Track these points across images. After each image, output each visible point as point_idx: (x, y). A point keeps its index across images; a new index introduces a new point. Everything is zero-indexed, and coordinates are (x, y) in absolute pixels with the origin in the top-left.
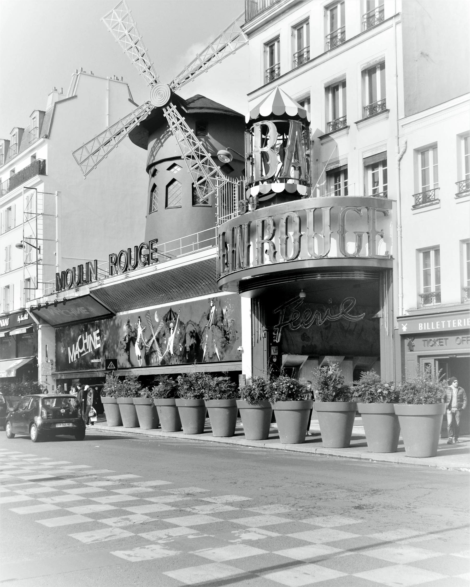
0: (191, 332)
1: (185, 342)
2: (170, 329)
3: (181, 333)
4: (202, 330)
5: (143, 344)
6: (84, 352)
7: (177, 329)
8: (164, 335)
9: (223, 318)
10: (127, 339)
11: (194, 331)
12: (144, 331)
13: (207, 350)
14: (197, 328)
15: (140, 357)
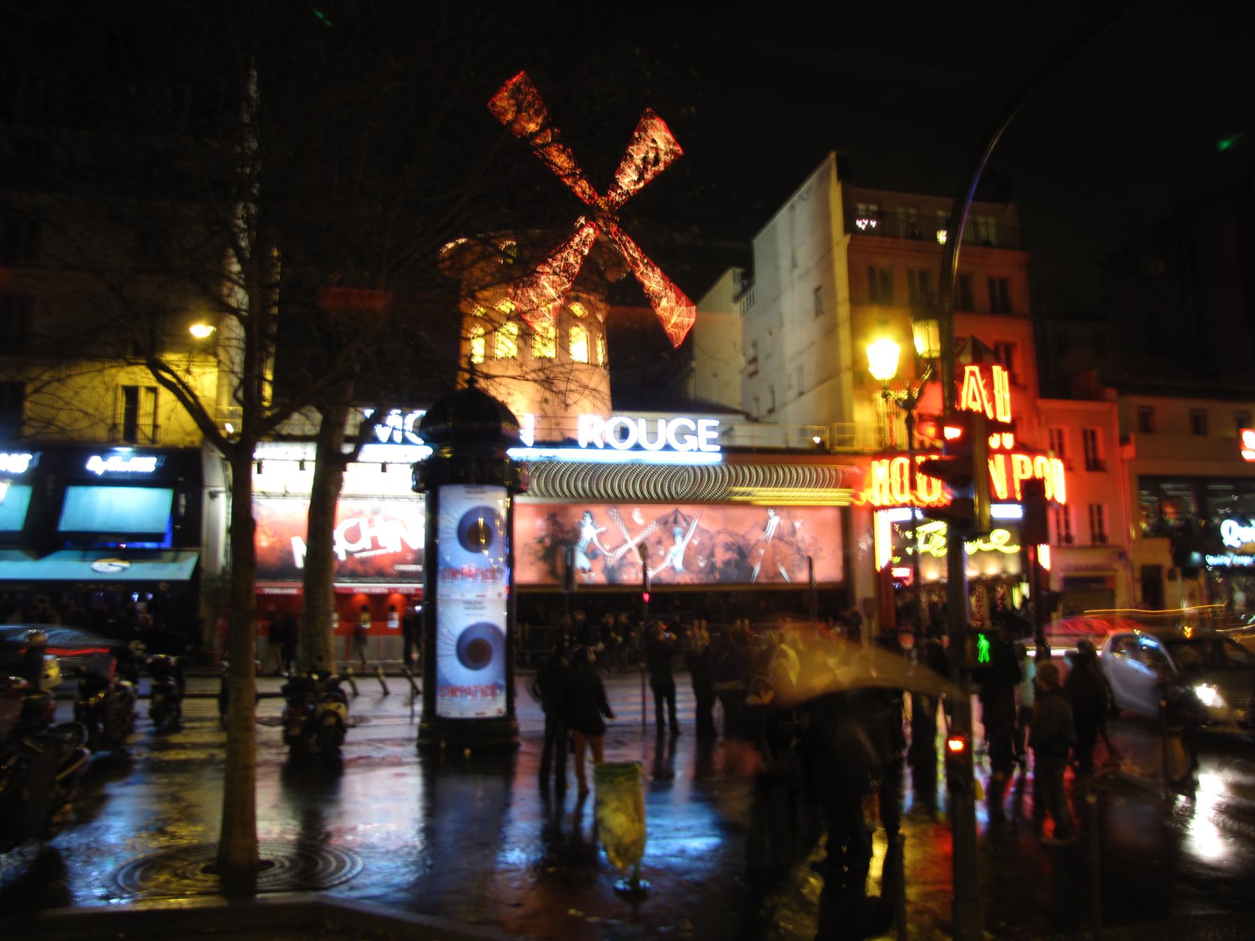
0: (726, 544)
1: (712, 555)
2: (674, 536)
3: (701, 543)
4: (752, 542)
5: (598, 552)
6: (363, 550)
7: (693, 537)
8: (659, 542)
9: (794, 532)
10: (548, 542)
11: (733, 544)
12: (601, 536)
13: (762, 567)
14: (741, 542)
15: (590, 571)
